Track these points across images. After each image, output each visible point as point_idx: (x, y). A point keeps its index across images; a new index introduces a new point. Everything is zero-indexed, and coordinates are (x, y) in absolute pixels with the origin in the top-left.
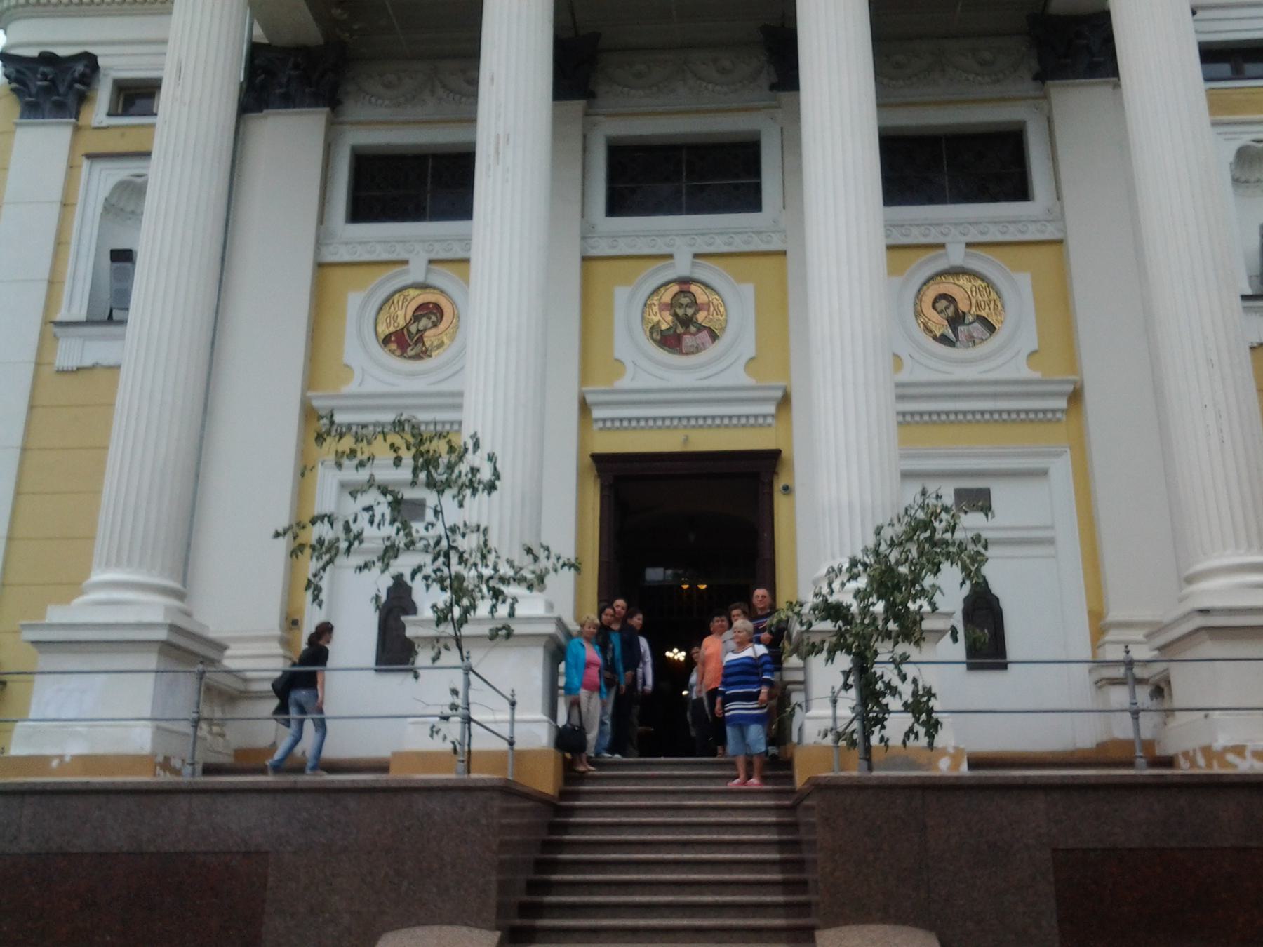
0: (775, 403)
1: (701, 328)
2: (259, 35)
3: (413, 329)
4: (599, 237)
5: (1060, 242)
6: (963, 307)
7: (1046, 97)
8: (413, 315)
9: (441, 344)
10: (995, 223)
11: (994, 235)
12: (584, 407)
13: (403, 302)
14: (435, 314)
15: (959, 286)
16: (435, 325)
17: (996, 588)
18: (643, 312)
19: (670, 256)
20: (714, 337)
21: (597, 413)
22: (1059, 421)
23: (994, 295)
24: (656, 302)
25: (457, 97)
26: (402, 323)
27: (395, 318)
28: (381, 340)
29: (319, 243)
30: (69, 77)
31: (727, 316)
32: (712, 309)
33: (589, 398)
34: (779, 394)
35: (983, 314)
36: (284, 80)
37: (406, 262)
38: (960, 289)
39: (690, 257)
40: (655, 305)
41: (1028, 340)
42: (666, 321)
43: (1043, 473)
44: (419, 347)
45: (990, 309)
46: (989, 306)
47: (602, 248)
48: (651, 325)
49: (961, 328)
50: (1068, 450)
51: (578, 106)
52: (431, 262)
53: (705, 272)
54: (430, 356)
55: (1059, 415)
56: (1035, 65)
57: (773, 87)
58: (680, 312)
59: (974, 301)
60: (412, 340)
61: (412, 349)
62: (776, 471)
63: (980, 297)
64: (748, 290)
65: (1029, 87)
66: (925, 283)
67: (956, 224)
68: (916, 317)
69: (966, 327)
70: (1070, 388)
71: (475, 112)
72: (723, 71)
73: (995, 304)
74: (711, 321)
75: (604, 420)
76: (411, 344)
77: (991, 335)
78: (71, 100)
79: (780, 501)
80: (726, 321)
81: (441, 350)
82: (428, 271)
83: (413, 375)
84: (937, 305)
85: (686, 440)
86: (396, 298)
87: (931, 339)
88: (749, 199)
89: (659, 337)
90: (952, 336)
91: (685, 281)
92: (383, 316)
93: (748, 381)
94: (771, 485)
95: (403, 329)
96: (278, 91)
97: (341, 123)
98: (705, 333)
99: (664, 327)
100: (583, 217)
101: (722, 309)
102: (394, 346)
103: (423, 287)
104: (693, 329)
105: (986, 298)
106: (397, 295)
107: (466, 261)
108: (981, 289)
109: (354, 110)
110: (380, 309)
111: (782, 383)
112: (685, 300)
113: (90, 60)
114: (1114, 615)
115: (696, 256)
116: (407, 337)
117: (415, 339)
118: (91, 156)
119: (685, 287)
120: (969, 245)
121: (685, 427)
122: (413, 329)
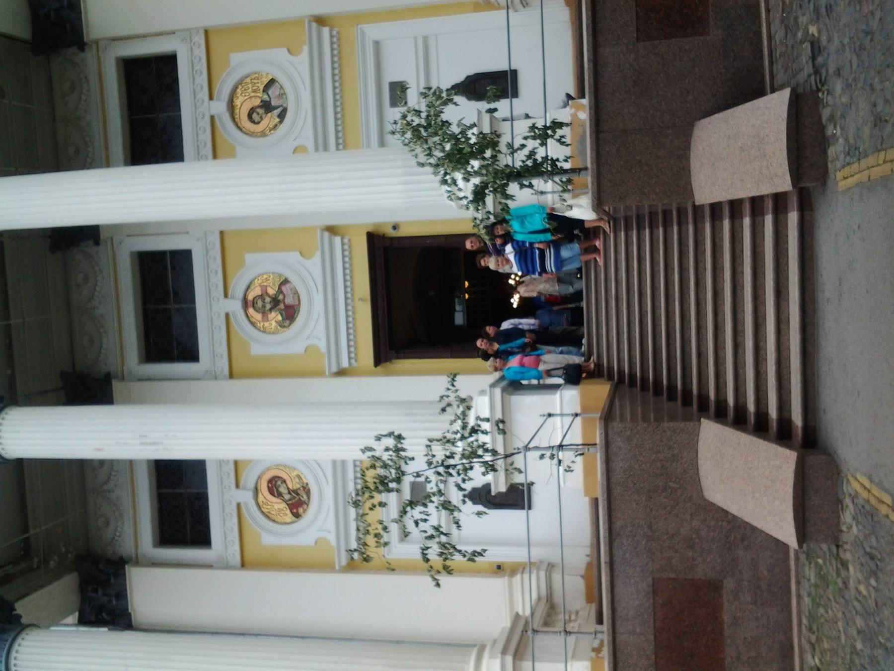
0: (333, 237)
1: (280, 291)
2: (73, 618)
4: (215, 366)
5: (206, 32)
6: (257, 102)
7: (97, 42)
8: (278, 497)
9: (299, 477)
10: (194, 79)
12: (341, 373)
13: (268, 505)
14: (276, 482)
15: (242, 105)
16: (284, 481)
17: (459, 78)
18: (270, 333)
19: (227, 315)
20: (286, 282)
21: (345, 364)
22: (338, 33)
23: (248, 80)
24: (262, 324)
25: (114, 473)
26: (284, 505)
27: (280, 510)
28: (296, 519)
29: (227, 567)
31: (270, 273)
32: (265, 284)
33: (334, 369)
34: (326, 234)
35: (262, 88)
36: (105, 599)
37: (239, 506)
38: (244, 105)
39: (226, 301)
40: (264, 325)
41: (280, 54)
42: (275, 317)
43: (377, 44)
44: (302, 492)
45: (258, 83)
46: (255, 84)
47: (223, 365)
48: (279, 328)
49: (273, 103)
50: (359, 26)
51: (117, 386)
52: (237, 486)
53: (238, 289)
54: (307, 484)
55: (334, 33)
56: (74, 49)
57: (97, 243)
58: (268, 306)
59: (252, 94)
60: (295, 497)
61: (302, 497)
62: (382, 235)
63: (250, 90)
64: (250, 258)
65: (89, 56)
66: (241, 130)
67: (196, 108)
68: (267, 135)
69: (272, 100)
70: (314, 25)
71: (124, 462)
72: (86, 279)
73: (255, 79)
74: (274, 284)
75: (350, 358)
76: (298, 498)
77: (277, 82)
79: (404, 232)
80: (273, 273)
81: (303, 477)
82: (245, 488)
83: (321, 494)
84: (256, 121)
85: (361, 300)
86: (265, 510)
87: (282, 125)
88: (182, 259)
89: (288, 322)
91: (245, 303)
92: (279, 519)
93: (318, 256)
94: (392, 239)
95: (288, 504)
96: (114, 602)
97: (137, 556)
98: (284, 288)
99: (280, 318)
100: (198, 379)
101: (265, 276)
102: (301, 510)
103: (256, 491)
104: (281, 297)
105: (250, 86)
106: (264, 510)
107: (236, 463)
108: (243, 89)
109: (126, 547)
110: (274, 521)
111: (318, 231)
112: (260, 303)
115: (226, 296)
116: (293, 501)
117: (296, 496)
119: (250, 304)
120: (211, 98)
121: (353, 300)
122: (287, 497)
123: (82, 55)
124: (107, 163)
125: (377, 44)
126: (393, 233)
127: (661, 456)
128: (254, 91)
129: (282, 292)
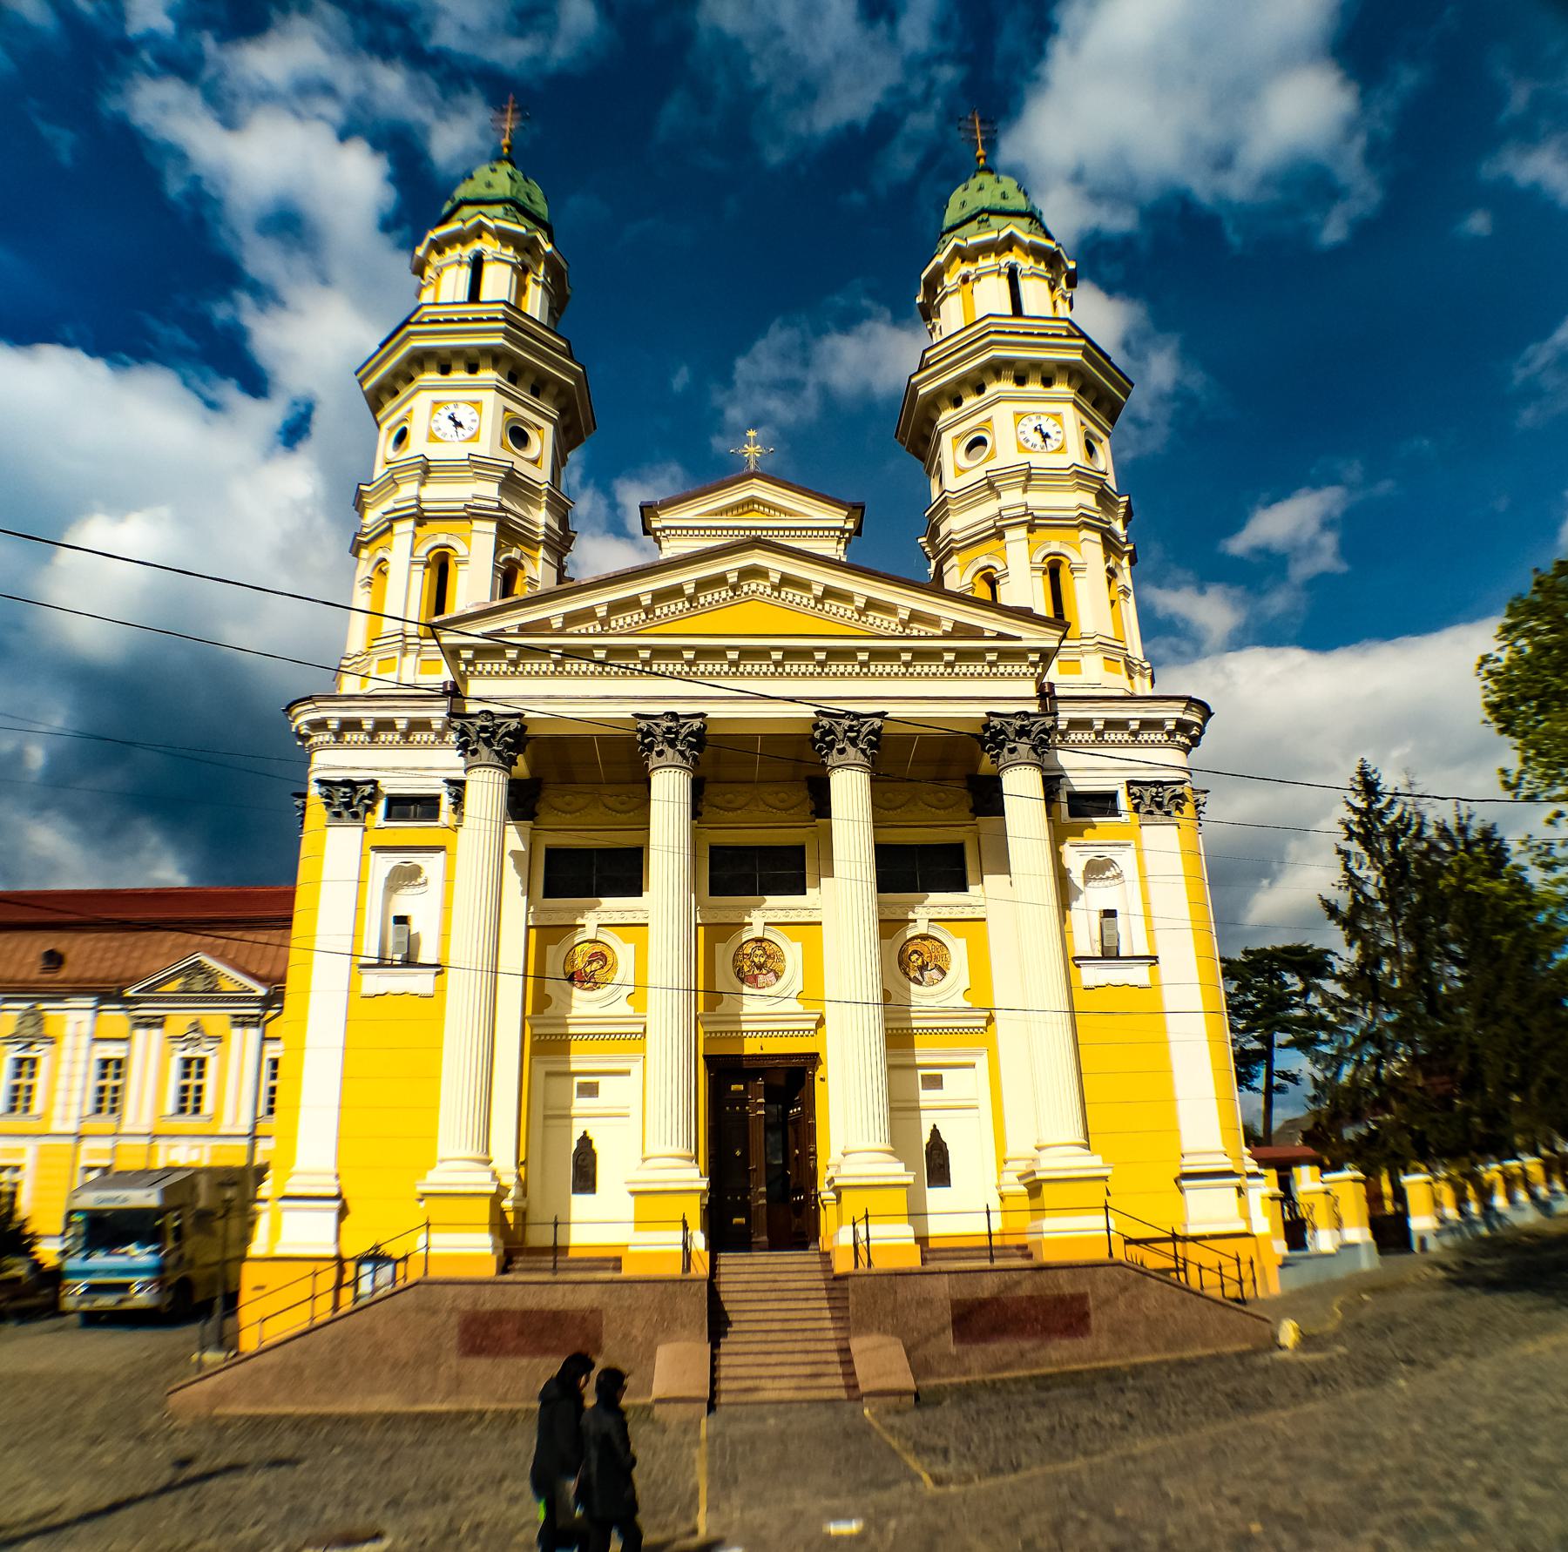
3: (588, 969)
11: (945, 914)
17: (944, 1137)
20: (778, 977)
30: (359, 796)
34: (818, 1016)
56: (972, 805)
58: (756, 960)
78: (361, 810)
90: (920, 978)
104: (764, 972)
109: (547, 818)
113: (374, 782)
114: (1008, 1156)
118: (378, 849)
119: (759, 944)
120: (930, 920)
122: (588, 969)
123: (967, 811)
124: (878, 823)
125: (973, 1066)
126: (818, 1075)
127: (685, 1317)
128: (936, 957)
129: (768, 972)
